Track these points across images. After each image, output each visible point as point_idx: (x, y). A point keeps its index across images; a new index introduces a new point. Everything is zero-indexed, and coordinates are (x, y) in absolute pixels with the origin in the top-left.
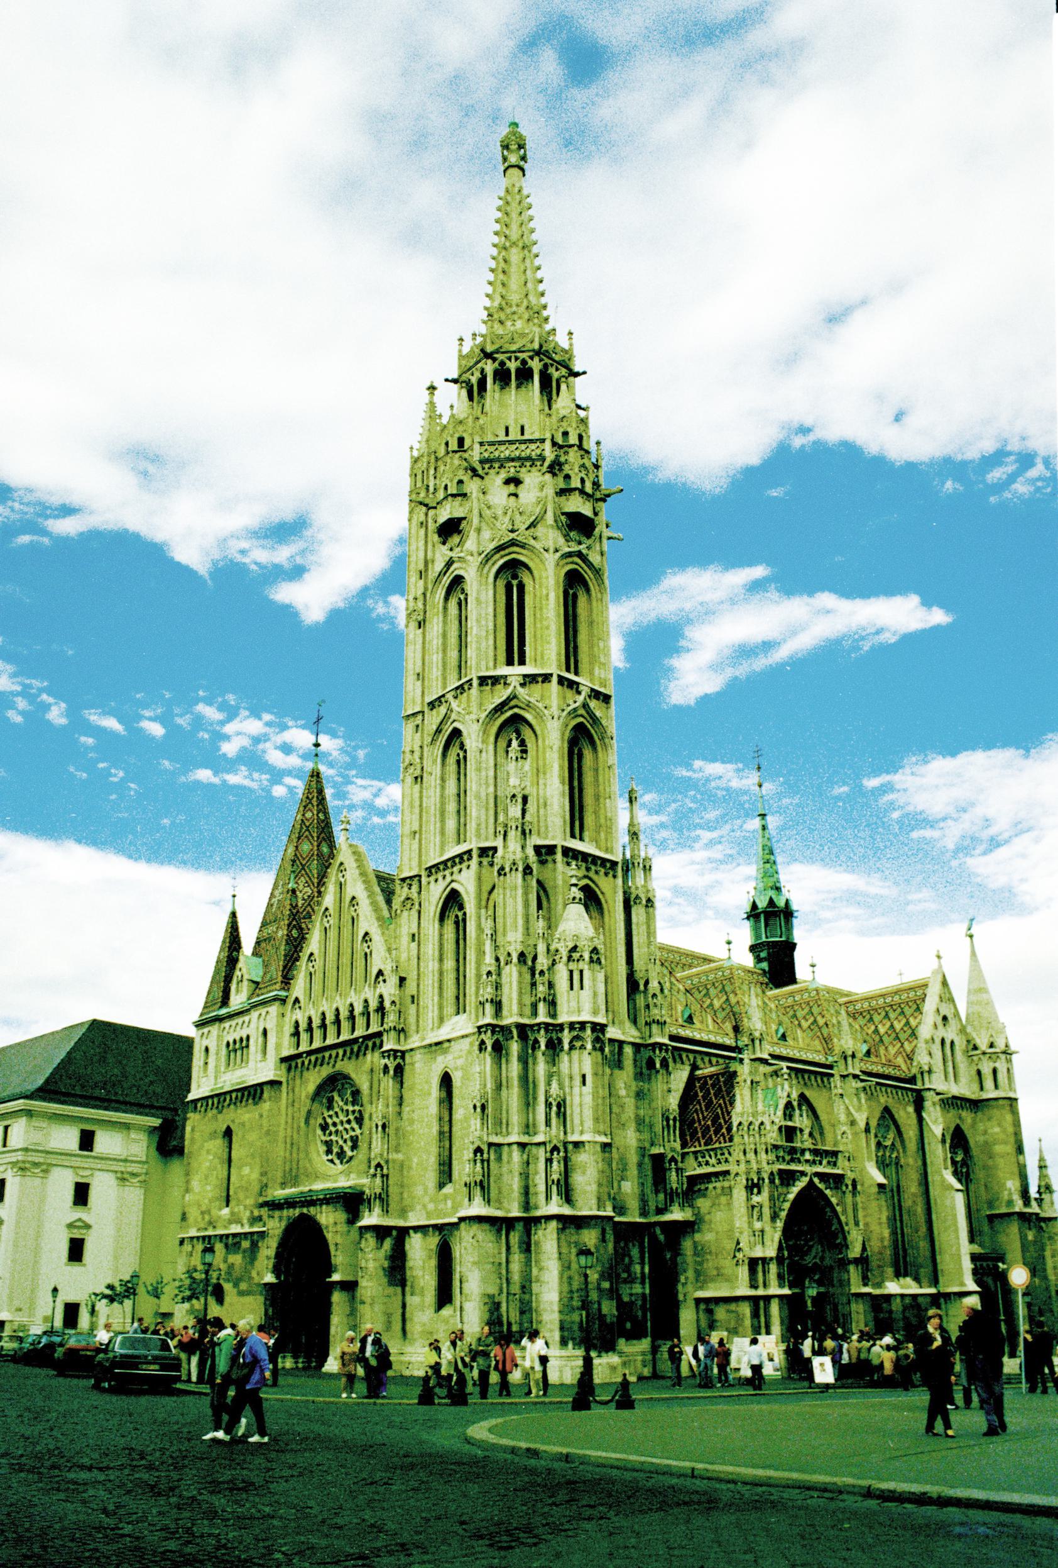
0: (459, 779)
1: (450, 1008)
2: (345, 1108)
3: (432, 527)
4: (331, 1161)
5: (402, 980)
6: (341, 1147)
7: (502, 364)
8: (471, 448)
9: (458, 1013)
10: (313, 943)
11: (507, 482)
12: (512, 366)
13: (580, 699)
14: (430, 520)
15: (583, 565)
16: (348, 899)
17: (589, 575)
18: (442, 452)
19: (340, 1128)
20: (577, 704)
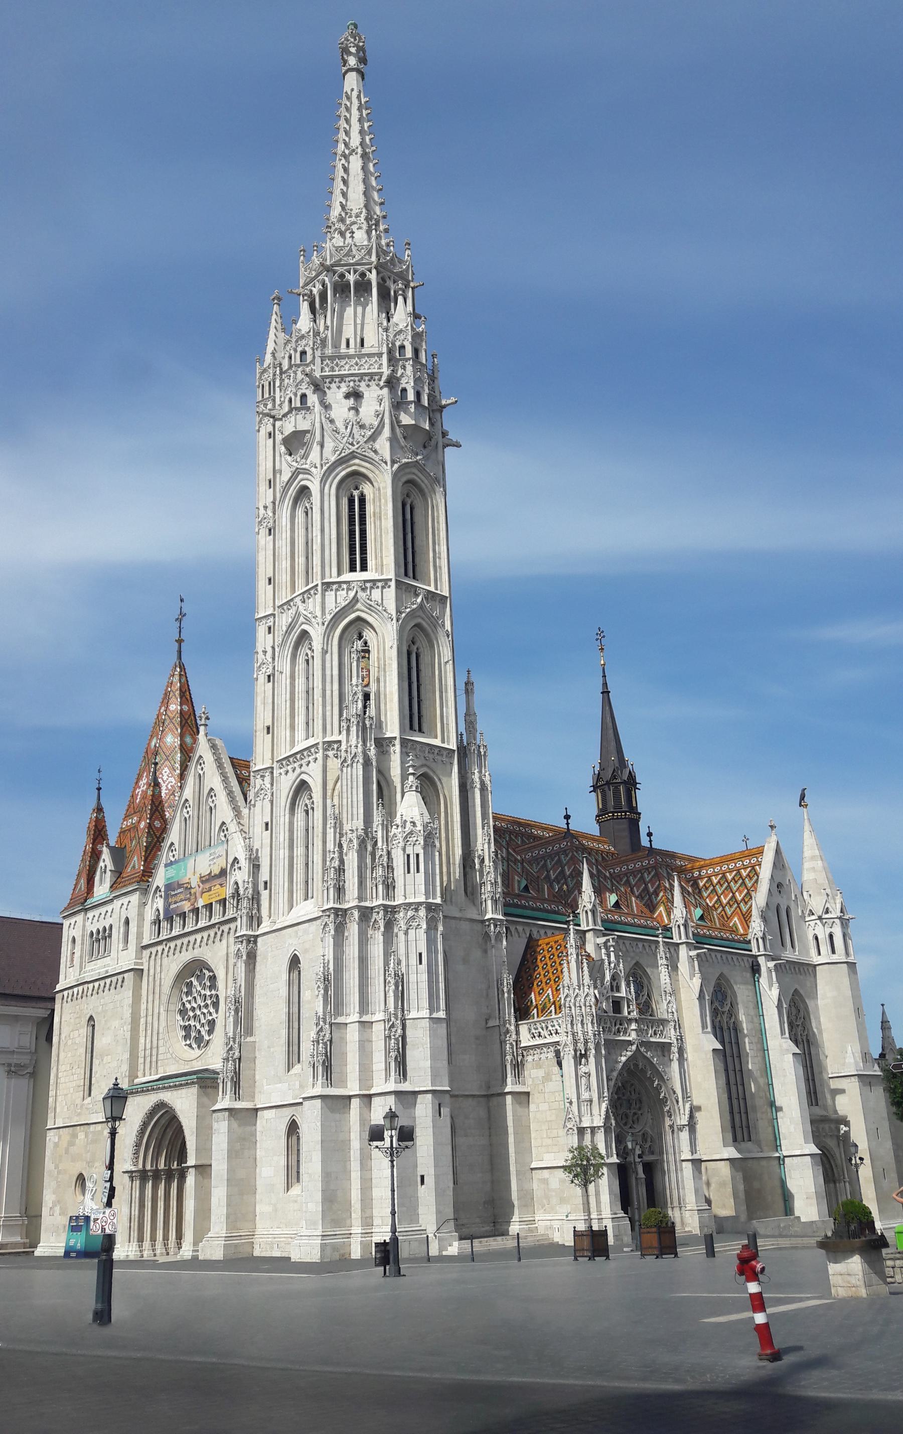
0: (308, 678)
1: (299, 894)
2: (203, 992)
3: (279, 437)
4: (190, 1046)
5: (255, 867)
6: (199, 1032)
7: (342, 276)
8: (313, 362)
9: (306, 899)
10: (174, 835)
11: (347, 396)
12: (351, 278)
13: (419, 600)
14: (277, 432)
15: (420, 475)
16: (206, 792)
18: (285, 366)
19: (198, 1013)
20: (415, 606)
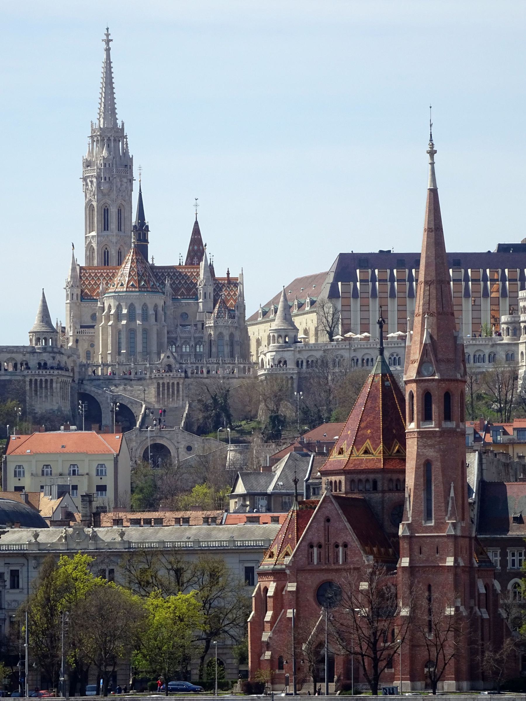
17: (109, 202)
